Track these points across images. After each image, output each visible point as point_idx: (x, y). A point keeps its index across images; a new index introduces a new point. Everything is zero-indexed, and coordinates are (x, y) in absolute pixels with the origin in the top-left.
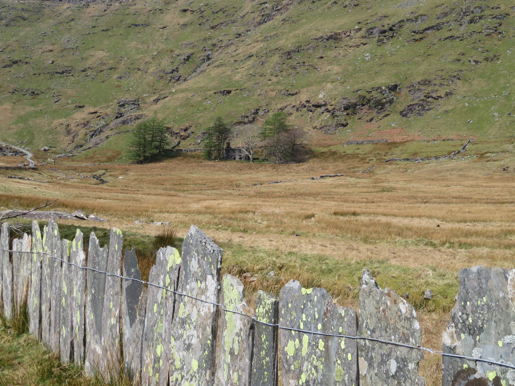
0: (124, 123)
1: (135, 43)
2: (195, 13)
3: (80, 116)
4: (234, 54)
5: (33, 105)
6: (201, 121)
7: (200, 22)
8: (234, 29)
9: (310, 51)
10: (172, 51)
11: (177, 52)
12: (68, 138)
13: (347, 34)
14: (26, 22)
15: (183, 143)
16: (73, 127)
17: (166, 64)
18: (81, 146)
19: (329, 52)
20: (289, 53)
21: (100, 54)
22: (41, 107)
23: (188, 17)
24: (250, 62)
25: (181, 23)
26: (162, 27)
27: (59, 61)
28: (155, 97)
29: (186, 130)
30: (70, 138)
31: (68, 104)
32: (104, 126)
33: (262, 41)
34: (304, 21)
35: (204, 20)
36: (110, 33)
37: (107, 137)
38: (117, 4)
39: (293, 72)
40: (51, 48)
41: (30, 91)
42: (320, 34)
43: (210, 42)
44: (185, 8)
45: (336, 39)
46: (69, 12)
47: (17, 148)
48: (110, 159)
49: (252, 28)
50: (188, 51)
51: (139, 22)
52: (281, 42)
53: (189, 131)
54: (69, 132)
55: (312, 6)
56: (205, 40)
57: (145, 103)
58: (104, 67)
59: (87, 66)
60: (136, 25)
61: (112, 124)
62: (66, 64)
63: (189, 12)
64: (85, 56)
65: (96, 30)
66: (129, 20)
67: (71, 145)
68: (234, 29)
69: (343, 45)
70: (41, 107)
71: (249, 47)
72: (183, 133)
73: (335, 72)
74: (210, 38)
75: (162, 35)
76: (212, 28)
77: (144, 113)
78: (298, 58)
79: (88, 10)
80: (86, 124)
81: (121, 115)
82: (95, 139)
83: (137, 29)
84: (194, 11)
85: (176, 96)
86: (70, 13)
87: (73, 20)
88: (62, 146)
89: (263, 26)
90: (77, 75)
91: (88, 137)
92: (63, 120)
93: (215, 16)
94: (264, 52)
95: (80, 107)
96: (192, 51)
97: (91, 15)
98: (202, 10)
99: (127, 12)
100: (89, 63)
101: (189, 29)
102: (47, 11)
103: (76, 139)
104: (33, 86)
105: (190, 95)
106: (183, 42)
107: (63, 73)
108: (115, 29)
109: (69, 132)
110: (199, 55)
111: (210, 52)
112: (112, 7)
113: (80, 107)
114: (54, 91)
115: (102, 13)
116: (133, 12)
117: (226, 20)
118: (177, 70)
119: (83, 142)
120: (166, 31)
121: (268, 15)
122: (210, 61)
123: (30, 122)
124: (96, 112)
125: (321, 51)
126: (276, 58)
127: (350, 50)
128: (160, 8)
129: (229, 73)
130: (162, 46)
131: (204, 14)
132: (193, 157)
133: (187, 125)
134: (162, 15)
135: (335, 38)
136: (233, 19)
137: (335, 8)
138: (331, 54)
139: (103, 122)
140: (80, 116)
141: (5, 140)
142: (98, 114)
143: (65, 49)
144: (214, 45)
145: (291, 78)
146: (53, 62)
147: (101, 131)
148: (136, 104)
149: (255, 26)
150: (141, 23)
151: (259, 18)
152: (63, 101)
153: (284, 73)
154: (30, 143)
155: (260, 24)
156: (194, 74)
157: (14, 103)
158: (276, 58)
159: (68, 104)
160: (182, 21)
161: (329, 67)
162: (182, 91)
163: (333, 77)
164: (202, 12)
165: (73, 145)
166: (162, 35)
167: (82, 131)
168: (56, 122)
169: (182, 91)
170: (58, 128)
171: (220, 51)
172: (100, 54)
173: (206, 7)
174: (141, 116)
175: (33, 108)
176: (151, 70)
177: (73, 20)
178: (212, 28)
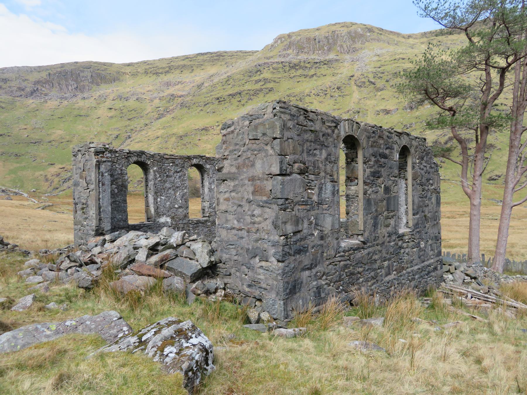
1: (81, 126)
3: (53, 170)
4: (146, 135)
5: (18, 163)
6: (135, 174)
8: (142, 122)
9: (193, 136)
10: (106, 132)
11: (109, 133)
12: (47, 183)
13: (212, 127)
14: (4, 110)
16: (49, 176)
18: (57, 189)
19: (203, 137)
20: (181, 137)
22: (23, 164)
23: (112, 113)
24: (158, 141)
27: (32, 135)
30: (48, 183)
31: (43, 162)
33: (162, 129)
34: (186, 119)
35: (124, 115)
36: (64, 120)
38: (66, 102)
39: (184, 147)
40: (25, 127)
41: (14, 154)
42: (197, 127)
43: (129, 128)
45: (206, 130)
46: (34, 105)
47: (14, 190)
49: (153, 121)
50: (116, 133)
51: (82, 114)
52: (175, 131)
54: (47, 180)
55: (188, 111)
56: (126, 126)
58: (63, 140)
59: (52, 139)
60: (80, 116)
62: (37, 137)
64: (49, 133)
65: (54, 117)
66: (76, 112)
67: (50, 188)
68: (142, 122)
69: (210, 133)
70: (23, 164)
71: (155, 132)
73: (209, 148)
75: (98, 122)
76: (129, 119)
78: (186, 140)
79: (47, 105)
80: (58, 175)
82: (66, 185)
83: (81, 118)
86: (35, 106)
87: (38, 110)
89: (160, 120)
90: (45, 144)
91: (61, 183)
92: (42, 172)
93: (130, 113)
94: (166, 135)
95: (52, 164)
96: (119, 133)
98: (122, 109)
99: (74, 107)
100: (52, 138)
101: (114, 120)
102: (18, 104)
103: (52, 184)
104: (16, 151)
106: (113, 127)
107: (35, 143)
109: (47, 180)
110: (124, 135)
111: (130, 134)
112: (63, 104)
113: (52, 164)
114: (31, 154)
115: (57, 107)
116: (77, 107)
119: (58, 186)
120: (100, 120)
121: (162, 114)
122: (131, 139)
123: (19, 174)
124: (64, 168)
125: (199, 136)
126: (173, 139)
127: (215, 136)
129: (146, 146)
130: (99, 129)
132: (135, 195)
135: (205, 129)
136: (142, 115)
137: (202, 113)
138: (204, 138)
139: (69, 174)
140: (53, 170)
141: (3, 185)
142: (65, 169)
143: (35, 128)
144: (132, 130)
145: (184, 151)
146: (28, 136)
149: (155, 120)
150: (83, 114)
151: (157, 116)
153: (179, 148)
154: (22, 187)
155: (157, 119)
157: (4, 161)
158: (173, 139)
159: (43, 162)
161: (205, 145)
163: (208, 151)
164: (122, 110)
166: (98, 122)
167: (56, 180)
170: (39, 177)
171: (136, 133)
175: (18, 165)
177: (38, 110)
178: (129, 119)
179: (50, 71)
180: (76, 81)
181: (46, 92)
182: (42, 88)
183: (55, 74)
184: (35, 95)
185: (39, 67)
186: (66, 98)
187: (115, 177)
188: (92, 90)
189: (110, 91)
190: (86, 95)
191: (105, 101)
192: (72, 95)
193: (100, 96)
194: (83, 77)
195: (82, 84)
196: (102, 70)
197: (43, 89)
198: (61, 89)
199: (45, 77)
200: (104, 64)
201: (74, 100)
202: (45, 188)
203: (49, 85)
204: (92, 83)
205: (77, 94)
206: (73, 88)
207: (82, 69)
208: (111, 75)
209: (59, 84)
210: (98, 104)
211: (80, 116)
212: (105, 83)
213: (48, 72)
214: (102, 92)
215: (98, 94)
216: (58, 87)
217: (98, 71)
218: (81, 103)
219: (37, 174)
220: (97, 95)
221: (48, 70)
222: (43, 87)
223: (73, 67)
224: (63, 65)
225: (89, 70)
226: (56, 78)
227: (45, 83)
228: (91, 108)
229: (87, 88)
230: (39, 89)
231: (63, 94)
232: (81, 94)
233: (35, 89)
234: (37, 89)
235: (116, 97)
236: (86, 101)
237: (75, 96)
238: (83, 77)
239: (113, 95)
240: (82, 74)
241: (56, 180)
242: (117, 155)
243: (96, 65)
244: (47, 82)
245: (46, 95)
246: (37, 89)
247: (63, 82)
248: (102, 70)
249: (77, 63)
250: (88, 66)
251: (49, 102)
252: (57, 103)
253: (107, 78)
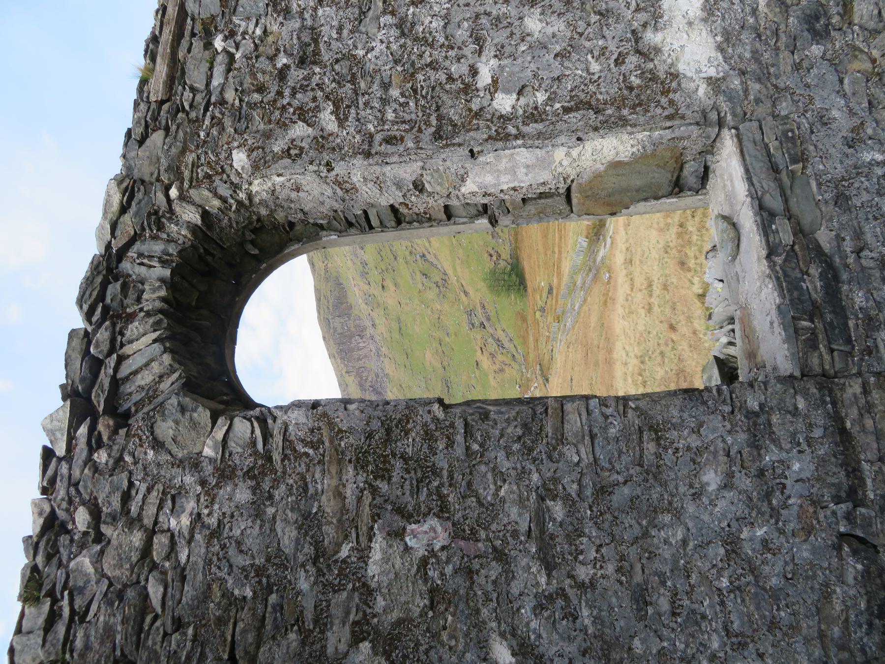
0: (488, 319)
3: (485, 363)
6: (481, 243)
10: (420, 292)
11: (420, 286)
12: (507, 370)
15: (503, 256)
17: (432, 294)
18: (514, 356)
21: (428, 356)
23: (389, 283)
28: (463, 295)
29: (491, 256)
30: (506, 369)
31: (475, 377)
32: (494, 338)
36: (409, 351)
37: (504, 331)
38: (383, 349)
43: (408, 258)
46: (395, 390)
48: (524, 319)
50: (419, 276)
53: (492, 252)
54: (502, 370)
56: (407, 263)
57: (469, 304)
58: (440, 350)
59: (440, 366)
60: (400, 329)
61: (491, 331)
62: (440, 384)
64: (431, 370)
65: (408, 364)
66: (396, 336)
72: (494, 258)
74: (405, 258)
75: (407, 304)
76: (396, 259)
77: (478, 301)
79: (391, 373)
80: (493, 356)
81: (482, 324)
82: (507, 344)
83: (403, 328)
85: (460, 274)
88: (515, 373)
92: (491, 378)
93: (385, 257)
95: (477, 364)
96: (418, 273)
99: (389, 339)
100: (438, 365)
101: (399, 280)
105: (458, 261)
109: (502, 370)
111: (418, 256)
113: (477, 364)
116: (389, 334)
118: (436, 283)
119: (509, 355)
122: (426, 253)
131: (384, 268)
132: (516, 240)
133: (486, 255)
139: (490, 340)
140: (485, 363)
142: (483, 346)
144: (411, 253)
147: (498, 340)
148: (470, 313)
152: (473, 382)
156: (439, 266)
159: (475, 377)
162: (455, 270)
165: (513, 364)
166: (407, 304)
167: (500, 358)
168: (493, 382)
169: (455, 270)
171: (415, 246)
172: (428, 356)
174: (481, 303)
176: (439, 307)
178: (396, 259)
179: (343, 372)
180: (351, 337)
181: (374, 376)
183: (346, 366)
184: (379, 389)
185: (340, 385)
186: (378, 350)
187: (287, 536)
188: (361, 315)
190: (368, 324)
193: (366, 304)
194: (343, 329)
195: (353, 329)
197: (370, 379)
198: (366, 356)
199: (353, 377)
200: (318, 300)
201: (377, 338)
202: (515, 373)
204: (349, 315)
205: (369, 336)
207: (332, 331)
209: (359, 359)
210: (379, 305)
211: (400, 329)
212: (345, 296)
214: (360, 301)
215: (363, 306)
218: (382, 329)
219: (493, 382)
221: (342, 375)
222: (366, 379)
223: (332, 342)
224: (332, 356)
227: (361, 377)
228: (387, 315)
231: (372, 353)
233: (371, 389)
236: (377, 322)
237: (372, 338)
238: (343, 329)
239: (361, 284)
240: (339, 330)
241: (500, 358)
242: (82, 518)
243: (322, 312)
245: (377, 376)
247: (355, 354)
249: (324, 338)
250: (325, 322)
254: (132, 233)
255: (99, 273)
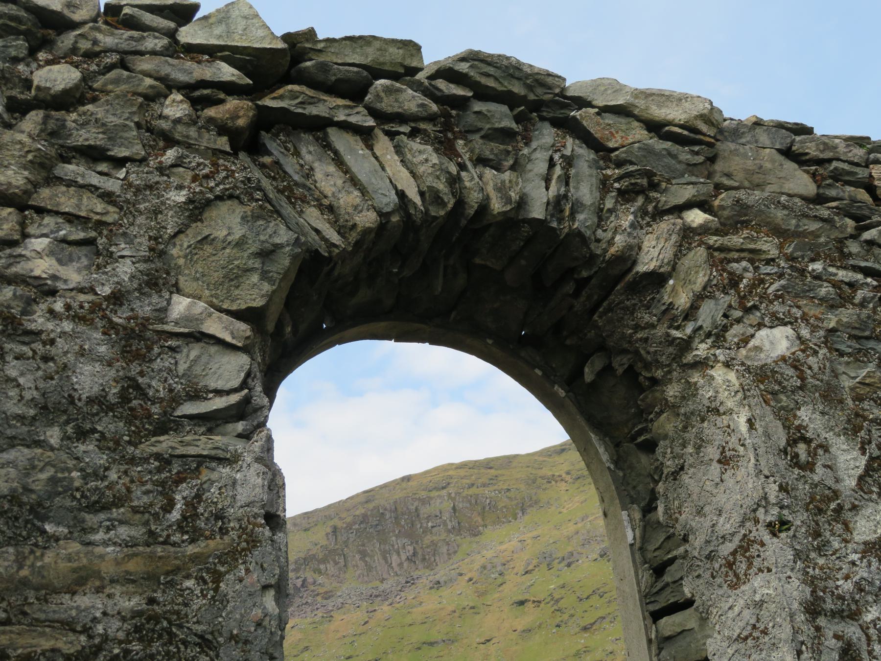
2: (542, 605)
7: (558, 620)
23: (529, 617)
25: (520, 628)
26: (483, 640)
35: (565, 617)
38: (385, 607)
44: (521, 598)
51: (435, 636)
60: (431, 644)
63: (530, 605)
76: (585, 629)
79: (333, 626)
83: (435, 651)
84: (539, 602)
86: (299, 636)
87: (306, 648)
93: (586, 604)
97: (339, 635)
98: (556, 596)
99: (408, 619)
108: (390, 656)
112: (378, 614)
117: (609, 610)
120: (492, 648)
128: (471, 604)
131: (562, 604)
134: (478, 617)
150: (439, 638)
160: (522, 623)
164: (557, 601)
173: (563, 591)
177: (306, 648)
178: (585, 629)
179: (336, 522)
180: (411, 535)
181: (328, 588)
182: (316, 576)
183: (349, 527)
186: (384, 596)
189: (514, 544)
190: (441, 574)
191: (500, 581)
192: (402, 580)
193: (484, 567)
194: (428, 518)
195: (427, 539)
196: (484, 485)
197: (320, 579)
198: (369, 568)
200: (488, 464)
203: (336, 563)
204: (458, 530)
205: (415, 574)
206: (404, 557)
207: (423, 494)
208: (511, 494)
209: (363, 554)
210: (482, 594)
212: (498, 521)
213: (331, 523)
214: (489, 554)
215: (479, 561)
216: (361, 564)
217: (471, 491)
218: (431, 602)
220: (477, 566)
222: (320, 573)
224: (369, 495)
225: (444, 492)
226: (352, 537)
227: (324, 561)
229: (444, 549)
230: (310, 580)
231: (377, 583)
232: (427, 572)
234: (304, 581)
235: (535, 562)
236: (445, 592)
237: (410, 582)
238: (428, 518)
240: (425, 511)
243: (462, 472)
244: (329, 555)
245: (328, 596)
246: (304, 581)
248: (484, 485)
249: (407, 479)
251: (338, 616)
252: (360, 615)
253: (501, 505)
254: (611, 145)
255: (530, 88)
